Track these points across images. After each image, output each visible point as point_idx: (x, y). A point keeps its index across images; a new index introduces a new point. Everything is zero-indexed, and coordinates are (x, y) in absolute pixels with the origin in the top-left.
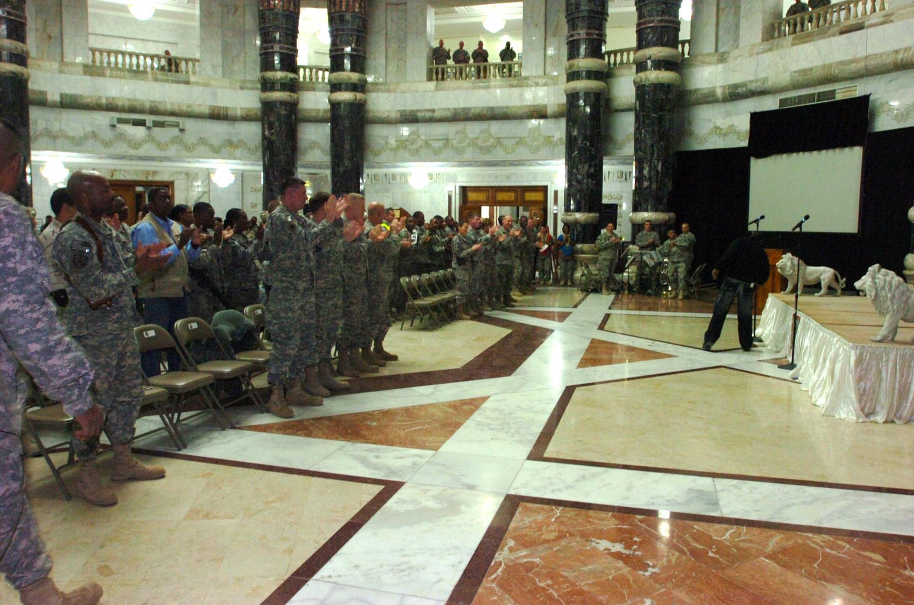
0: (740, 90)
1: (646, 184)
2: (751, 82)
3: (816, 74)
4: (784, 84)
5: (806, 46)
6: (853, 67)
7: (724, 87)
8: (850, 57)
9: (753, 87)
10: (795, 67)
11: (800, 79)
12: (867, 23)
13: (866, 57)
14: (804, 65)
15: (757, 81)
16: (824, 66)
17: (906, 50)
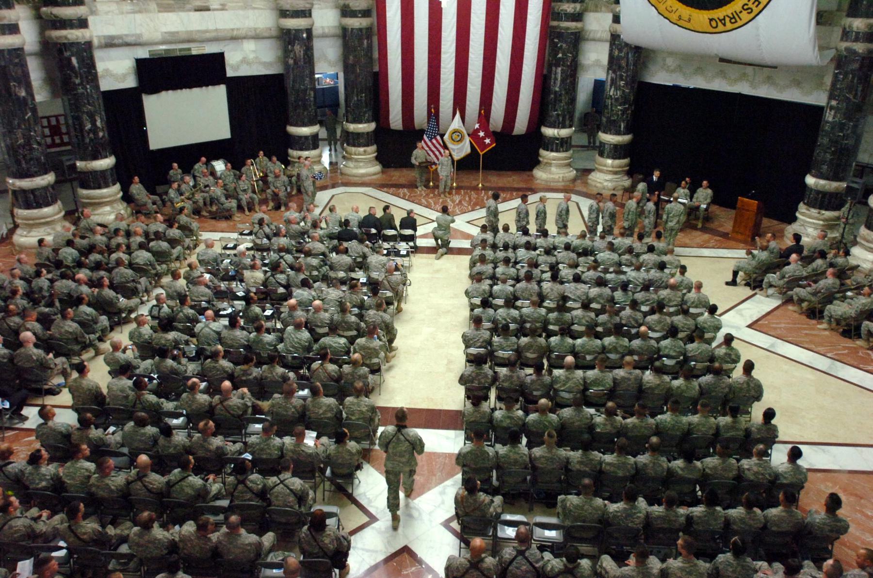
0: (116, 41)
1: (101, 134)
2: (126, 35)
3: (183, 36)
4: (156, 41)
5: (170, 14)
6: (208, 35)
7: (98, 37)
8: (203, 28)
9: (129, 40)
10: (164, 30)
11: (169, 38)
12: (211, 7)
13: (216, 30)
14: (173, 29)
15: (133, 35)
16: (187, 32)
17: (238, 29)
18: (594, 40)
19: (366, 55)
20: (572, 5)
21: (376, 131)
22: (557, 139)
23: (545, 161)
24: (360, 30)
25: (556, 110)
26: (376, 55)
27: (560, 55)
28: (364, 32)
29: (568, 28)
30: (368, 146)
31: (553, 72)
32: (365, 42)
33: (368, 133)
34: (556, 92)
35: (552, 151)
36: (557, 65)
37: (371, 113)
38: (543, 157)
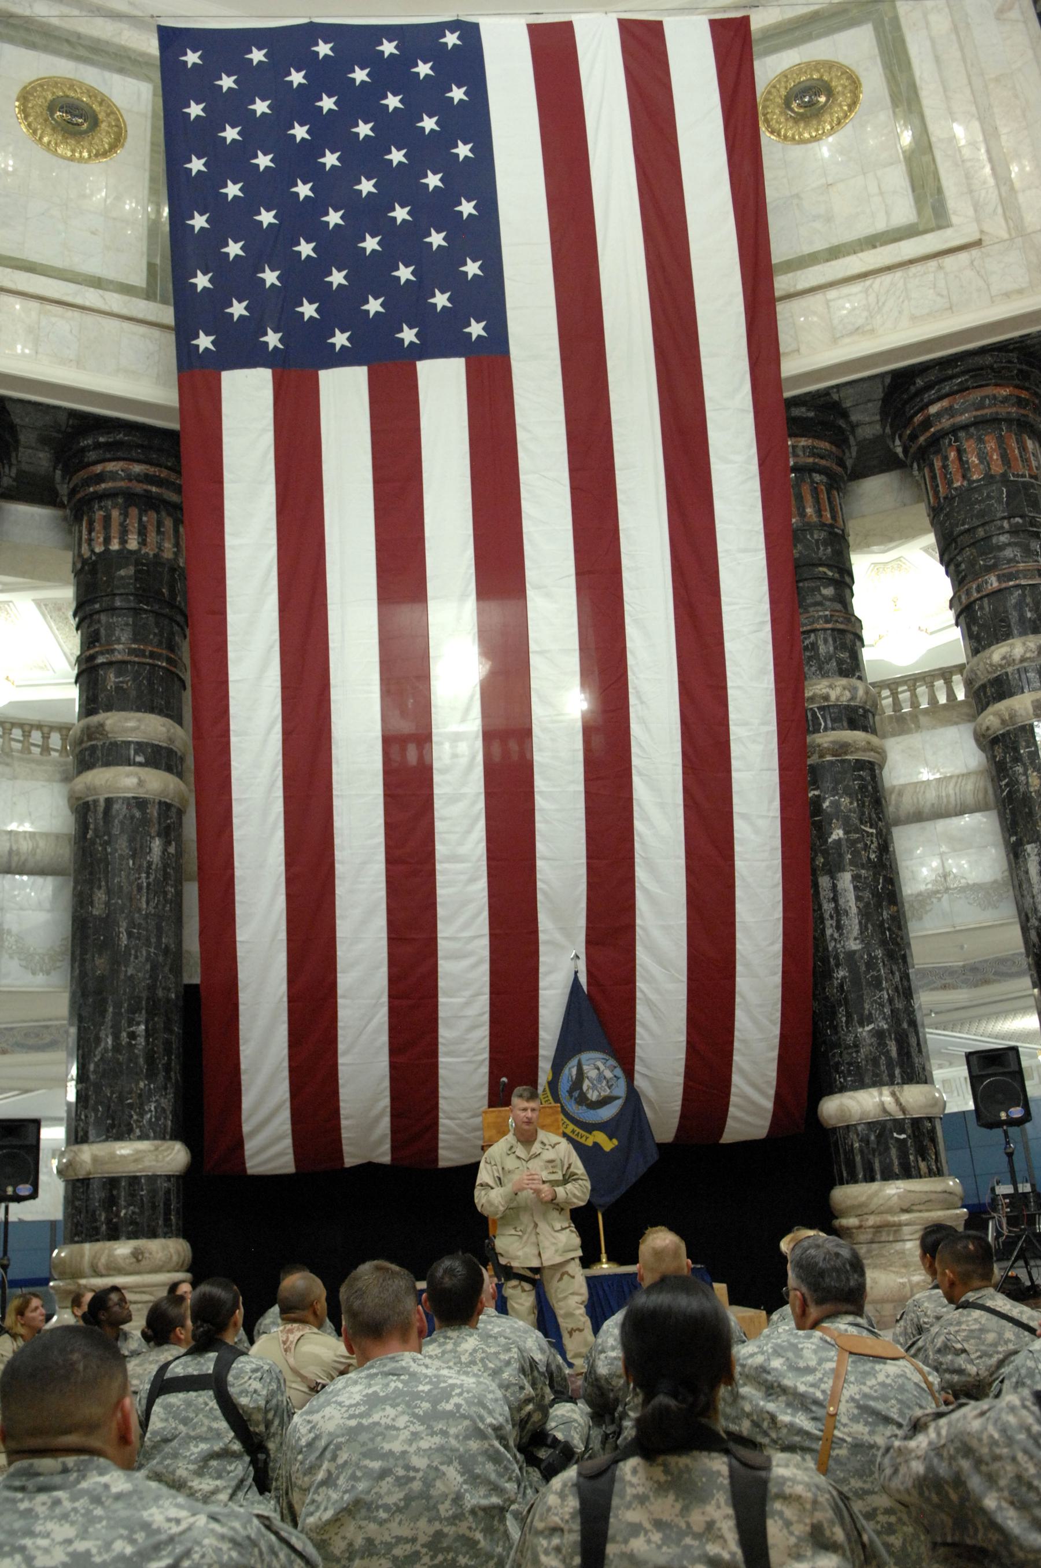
18: (918, 817)
19: (157, 889)
20: (844, 681)
21: (188, 1180)
22: (898, 1125)
23: (872, 1220)
24: (141, 803)
25: (870, 1019)
26: (192, 943)
27: (838, 834)
28: (154, 812)
29: (844, 747)
30: (153, 1235)
31: (825, 892)
32: (157, 844)
33: (153, 1179)
34: (850, 955)
35: (888, 1176)
36: (833, 870)
37: (167, 1103)
38: (860, 1209)
